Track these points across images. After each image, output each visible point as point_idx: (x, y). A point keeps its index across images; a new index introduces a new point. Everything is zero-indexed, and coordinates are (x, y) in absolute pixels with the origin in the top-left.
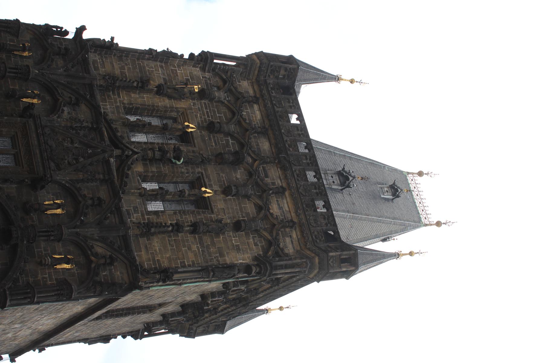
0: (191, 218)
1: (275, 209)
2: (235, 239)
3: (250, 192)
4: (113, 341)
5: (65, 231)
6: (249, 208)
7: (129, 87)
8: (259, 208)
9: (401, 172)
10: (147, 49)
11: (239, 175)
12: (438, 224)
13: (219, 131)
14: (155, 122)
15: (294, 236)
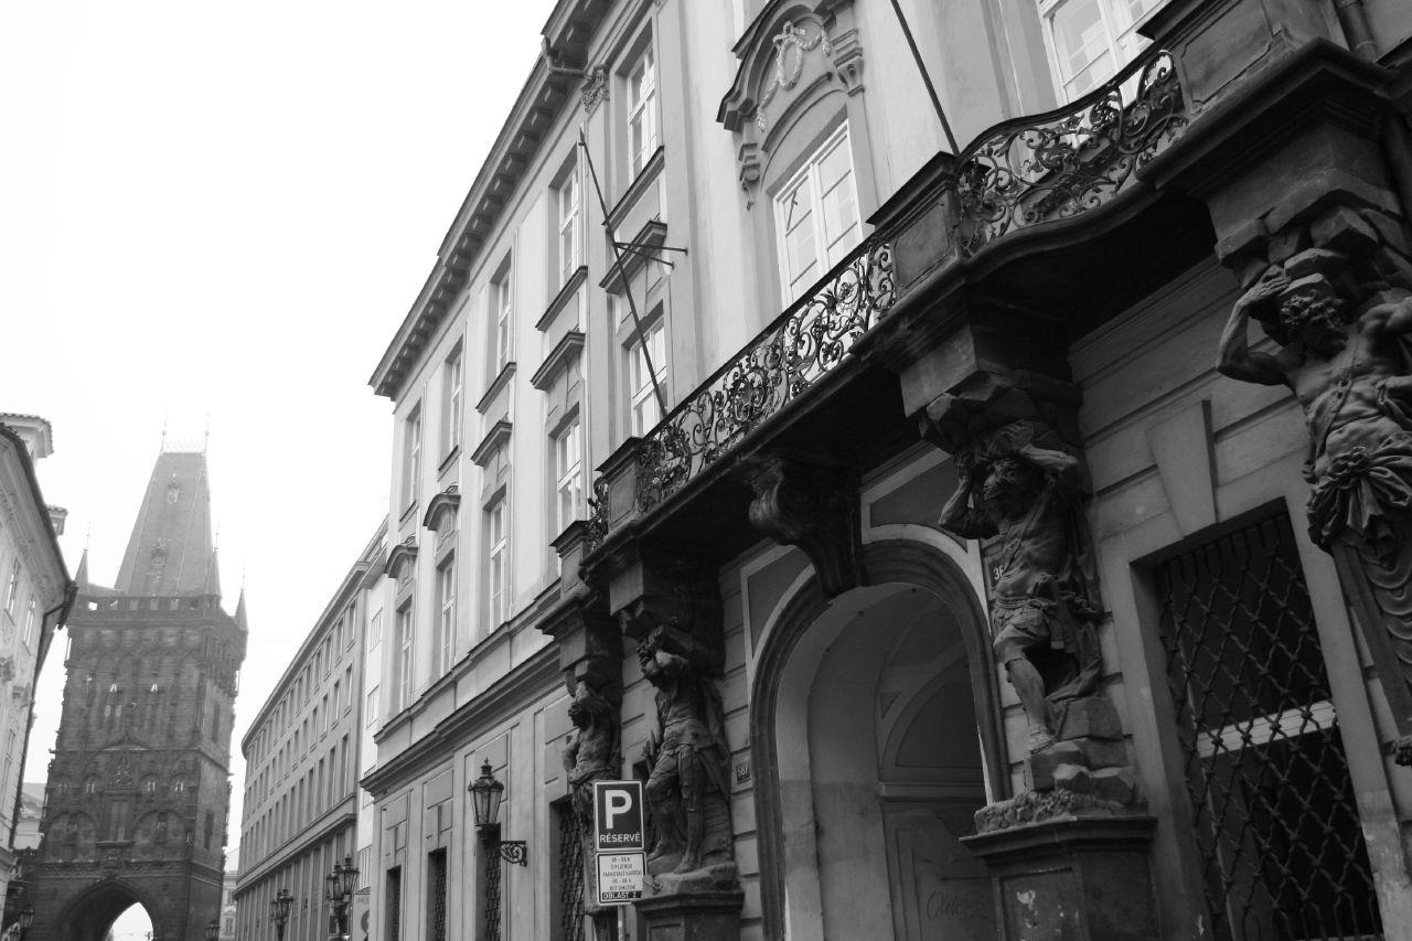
0: (168, 703)
1: (171, 641)
2: (185, 677)
3: (157, 658)
4: (235, 712)
5: (165, 784)
6: (167, 661)
7: (87, 726)
8: (169, 654)
9: (160, 458)
10: (61, 707)
11: (147, 662)
12: (207, 434)
13: (117, 670)
14: (108, 709)
15: (188, 631)
